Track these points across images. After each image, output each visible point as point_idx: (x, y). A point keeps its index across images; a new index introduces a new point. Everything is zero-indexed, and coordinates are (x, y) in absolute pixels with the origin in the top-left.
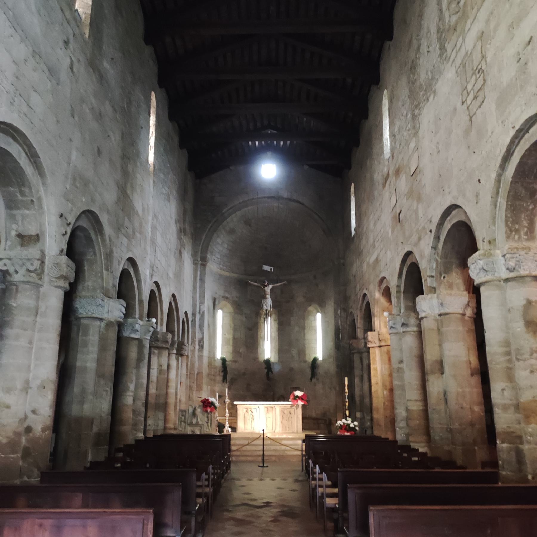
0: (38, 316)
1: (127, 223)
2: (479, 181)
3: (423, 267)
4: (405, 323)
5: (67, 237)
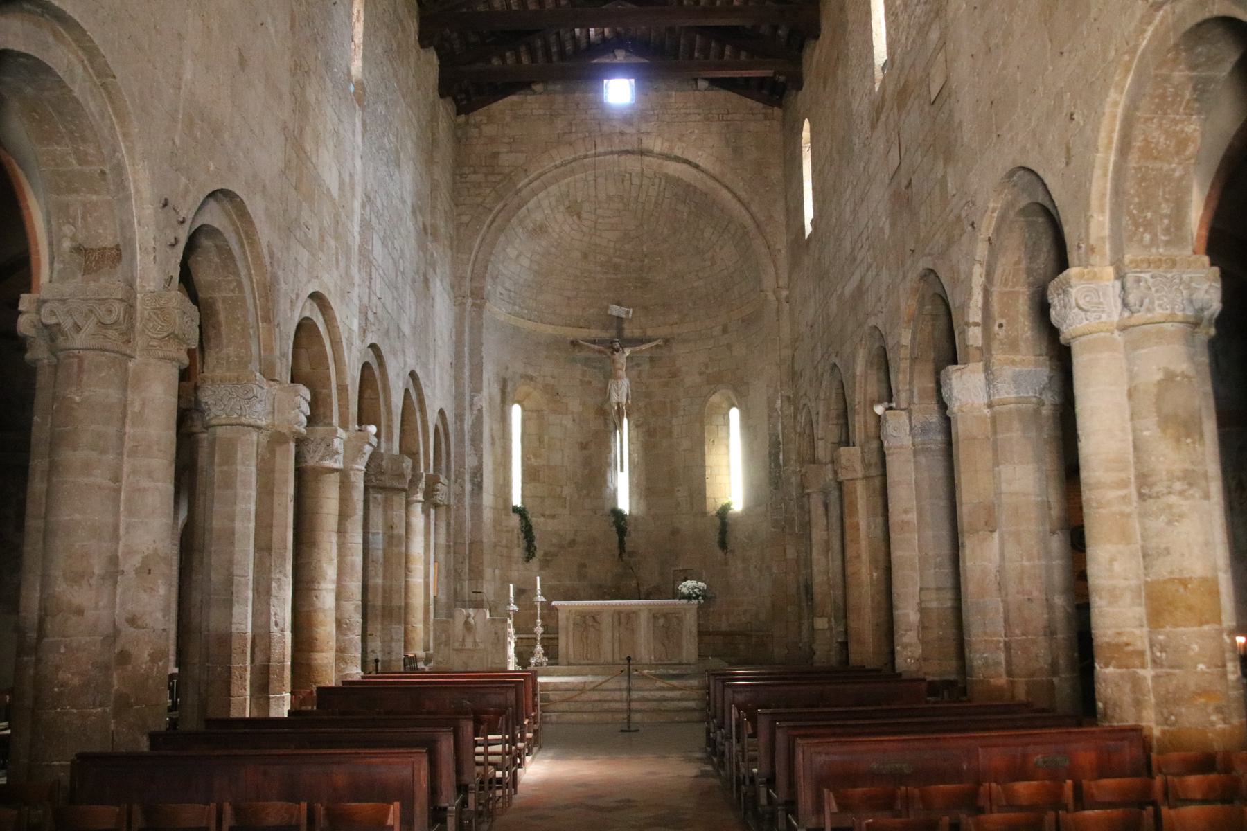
0: (128, 421)
1: (305, 215)
2: (1072, 115)
3: (957, 305)
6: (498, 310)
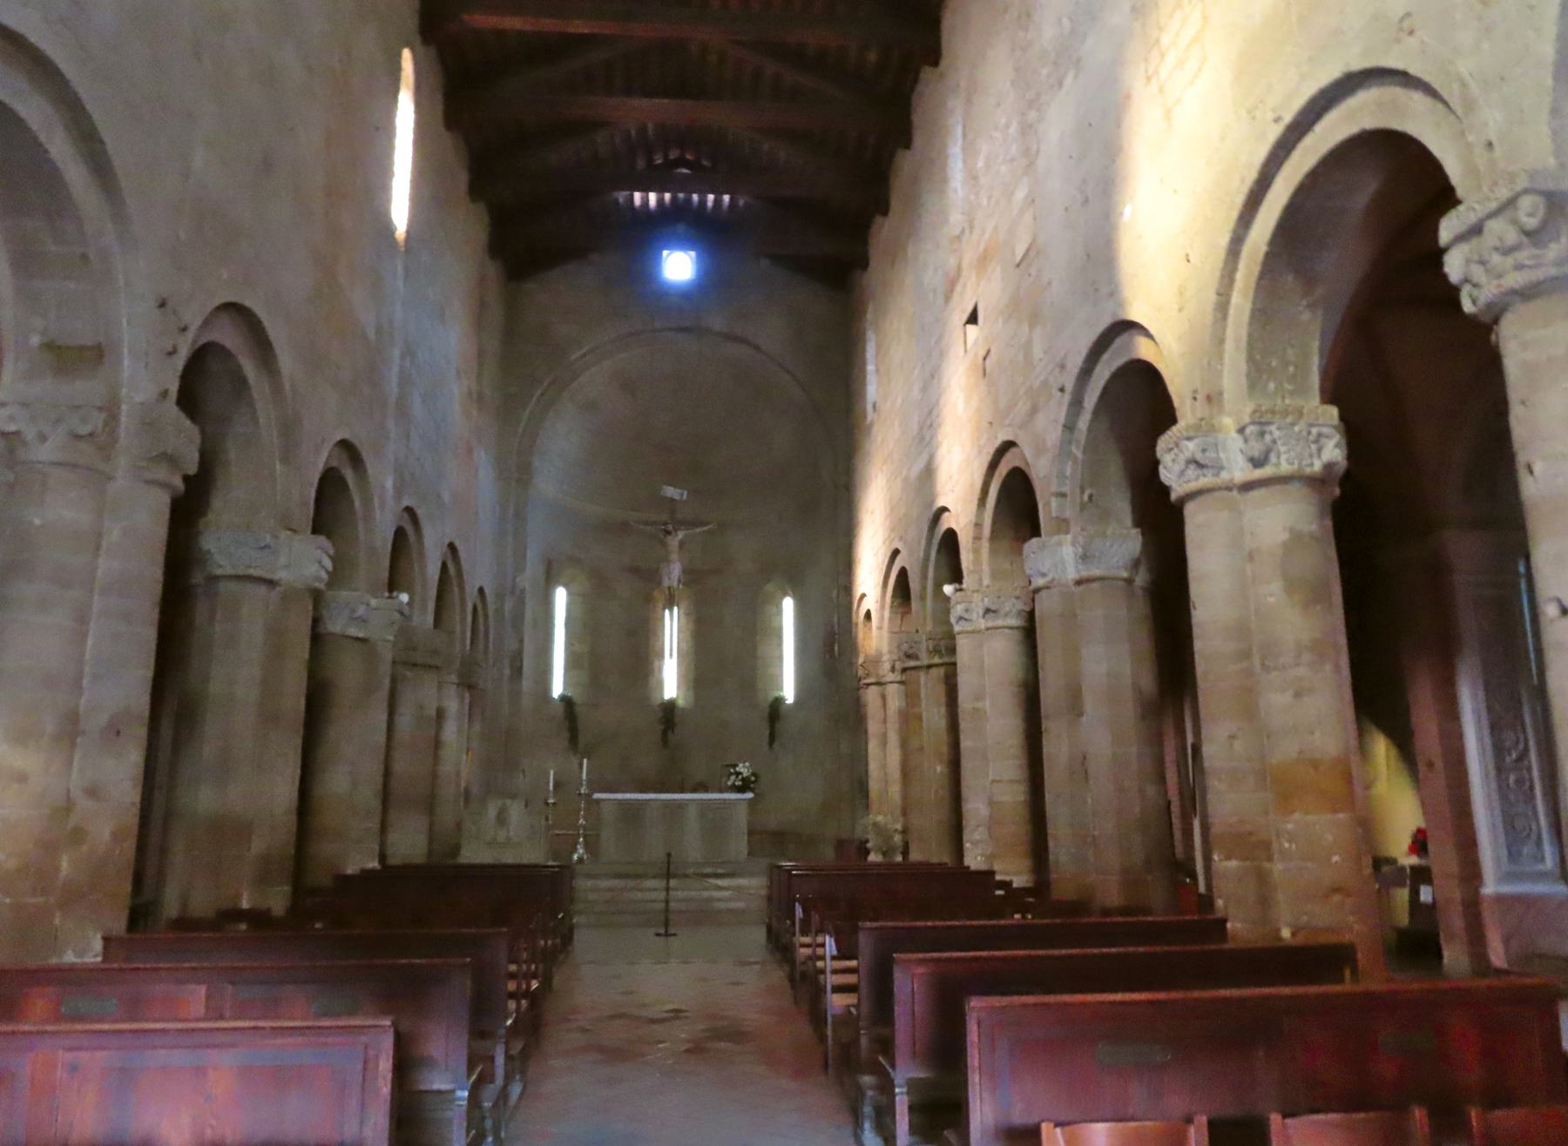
4: (993, 608)
6: (548, 483)
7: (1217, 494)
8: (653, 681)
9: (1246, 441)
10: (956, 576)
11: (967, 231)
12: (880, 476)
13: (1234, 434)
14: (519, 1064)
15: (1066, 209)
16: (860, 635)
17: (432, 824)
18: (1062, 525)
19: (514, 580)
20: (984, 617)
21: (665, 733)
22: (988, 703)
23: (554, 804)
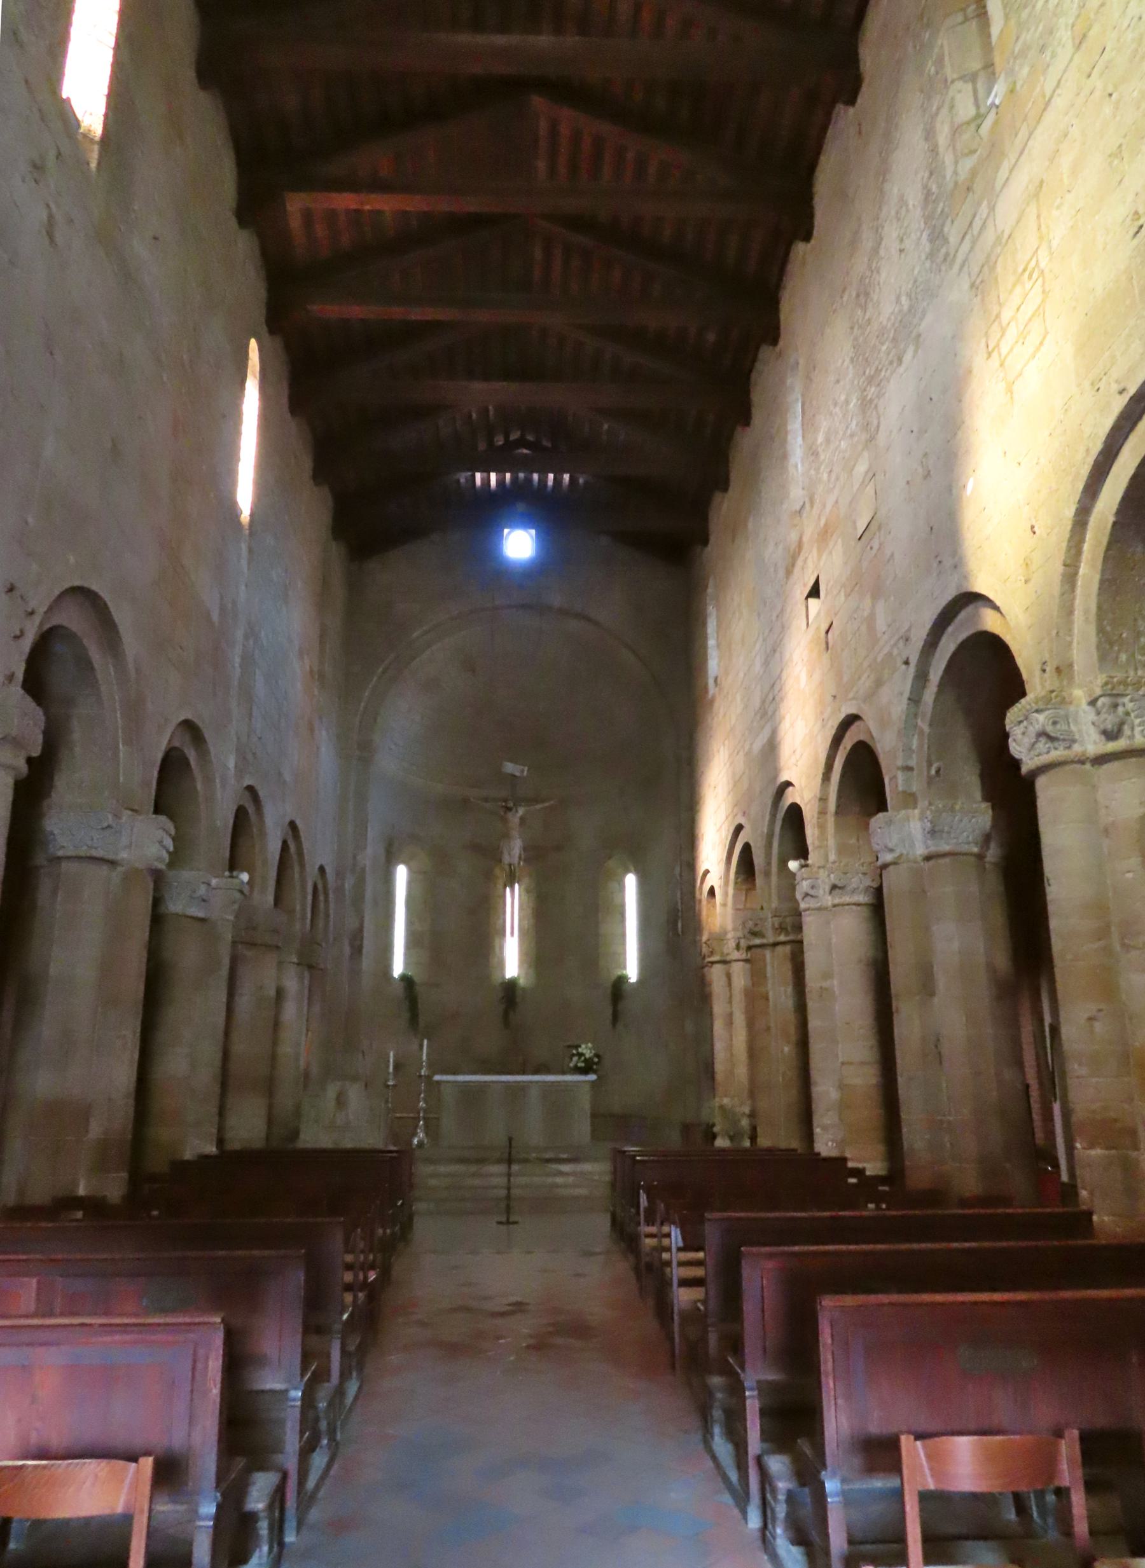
5: (27, 644)
7: (1067, 768)
8: (494, 961)
9: (1098, 713)
10: (802, 852)
11: (807, 506)
12: (722, 748)
13: (1084, 706)
14: (355, 1361)
15: (908, 483)
16: (704, 913)
17: (270, 1107)
18: (910, 800)
19: (355, 857)
20: (830, 893)
21: (506, 1015)
22: (835, 982)
23: (394, 1086)
